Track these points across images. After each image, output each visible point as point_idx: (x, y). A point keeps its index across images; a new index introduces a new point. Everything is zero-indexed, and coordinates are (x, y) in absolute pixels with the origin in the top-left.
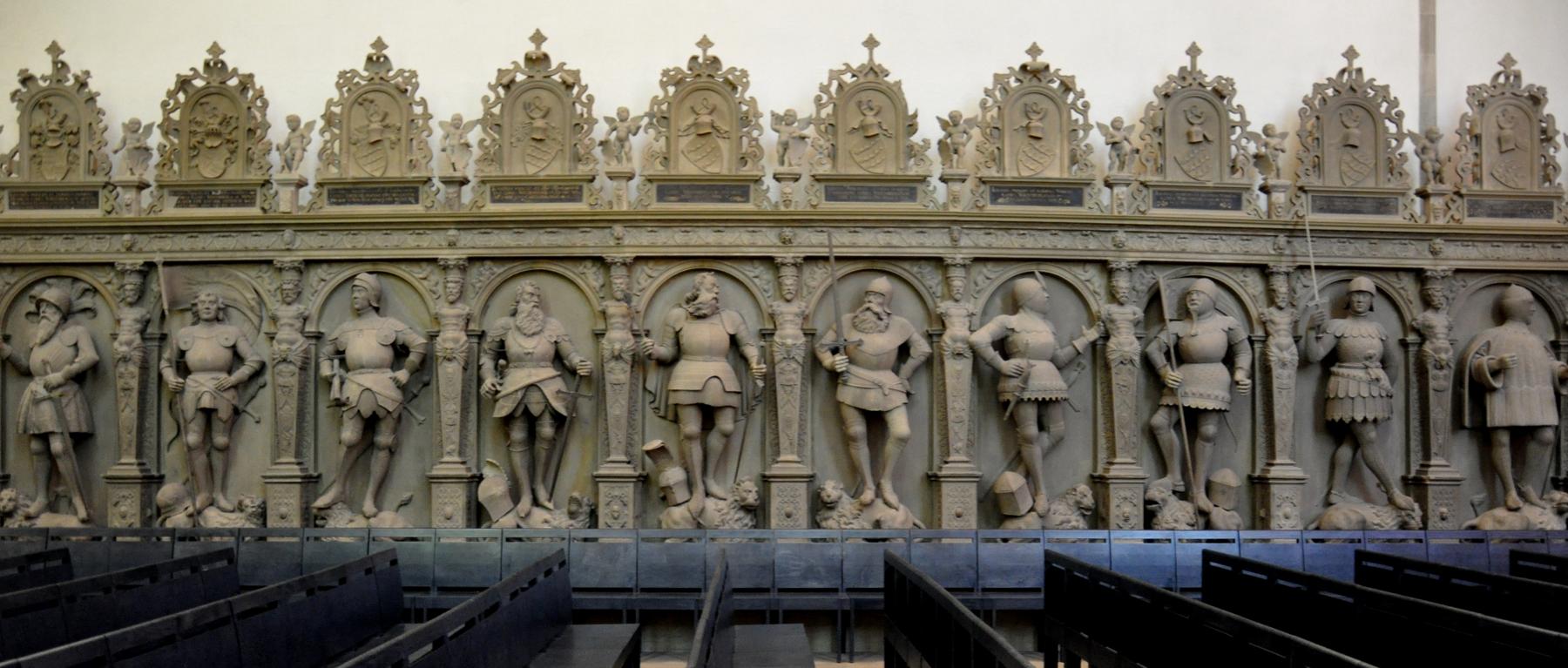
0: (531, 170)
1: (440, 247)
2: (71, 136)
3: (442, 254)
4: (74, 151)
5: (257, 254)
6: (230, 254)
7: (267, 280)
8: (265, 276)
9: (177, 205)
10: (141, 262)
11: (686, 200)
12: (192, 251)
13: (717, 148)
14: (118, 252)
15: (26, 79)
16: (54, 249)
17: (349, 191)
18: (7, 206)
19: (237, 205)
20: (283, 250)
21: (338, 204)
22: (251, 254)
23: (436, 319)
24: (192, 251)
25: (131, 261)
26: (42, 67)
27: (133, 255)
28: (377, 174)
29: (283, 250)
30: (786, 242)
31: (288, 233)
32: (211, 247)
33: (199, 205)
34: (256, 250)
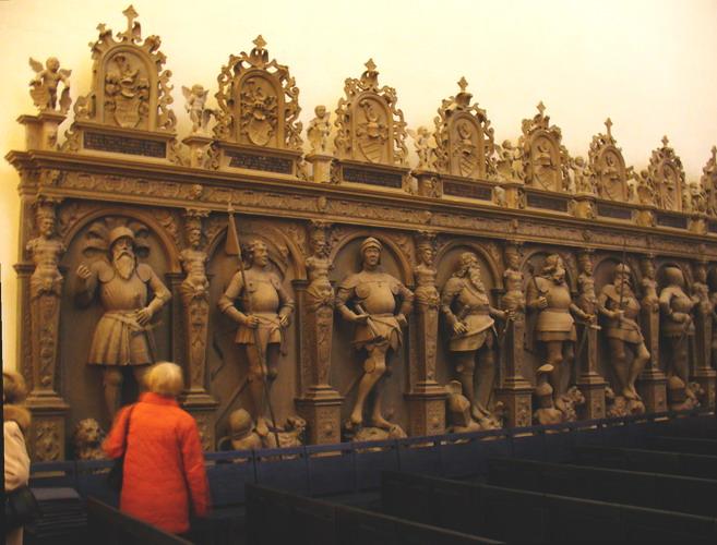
0: (465, 175)
1: (420, 223)
2: (144, 91)
3: (421, 229)
4: (144, 104)
5: (298, 214)
6: (276, 211)
7: (296, 238)
8: (296, 232)
9: (231, 165)
10: (210, 211)
11: (540, 207)
12: (250, 205)
13: (551, 176)
14: (187, 199)
15: (105, 36)
16: (128, 191)
17: (358, 171)
18: (82, 146)
19: (278, 171)
20: (314, 212)
21: (350, 181)
22: (294, 213)
23: (416, 277)
24: (250, 205)
25: (199, 209)
26: (119, 26)
27: (200, 204)
28: (375, 161)
29: (314, 212)
30: (587, 239)
31: (323, 201)
32: (263, 204)
33: (249, 167)
34: (298, 210)
